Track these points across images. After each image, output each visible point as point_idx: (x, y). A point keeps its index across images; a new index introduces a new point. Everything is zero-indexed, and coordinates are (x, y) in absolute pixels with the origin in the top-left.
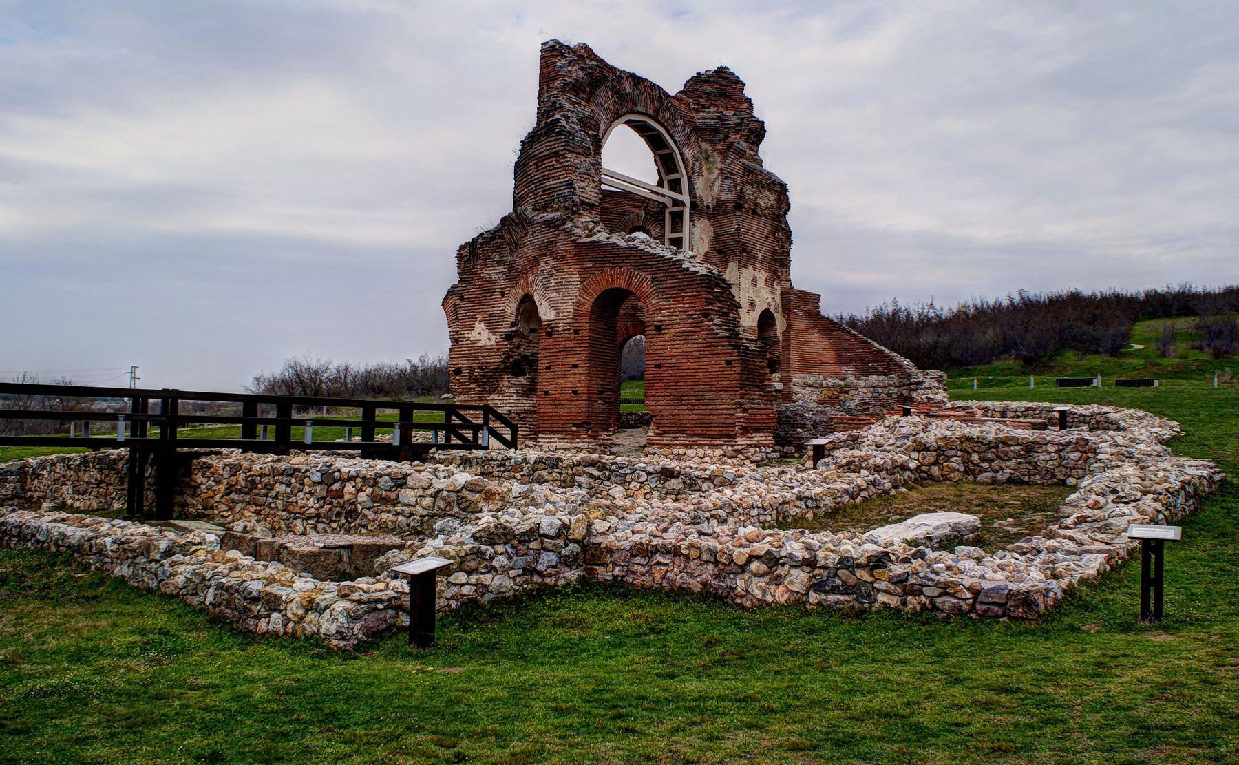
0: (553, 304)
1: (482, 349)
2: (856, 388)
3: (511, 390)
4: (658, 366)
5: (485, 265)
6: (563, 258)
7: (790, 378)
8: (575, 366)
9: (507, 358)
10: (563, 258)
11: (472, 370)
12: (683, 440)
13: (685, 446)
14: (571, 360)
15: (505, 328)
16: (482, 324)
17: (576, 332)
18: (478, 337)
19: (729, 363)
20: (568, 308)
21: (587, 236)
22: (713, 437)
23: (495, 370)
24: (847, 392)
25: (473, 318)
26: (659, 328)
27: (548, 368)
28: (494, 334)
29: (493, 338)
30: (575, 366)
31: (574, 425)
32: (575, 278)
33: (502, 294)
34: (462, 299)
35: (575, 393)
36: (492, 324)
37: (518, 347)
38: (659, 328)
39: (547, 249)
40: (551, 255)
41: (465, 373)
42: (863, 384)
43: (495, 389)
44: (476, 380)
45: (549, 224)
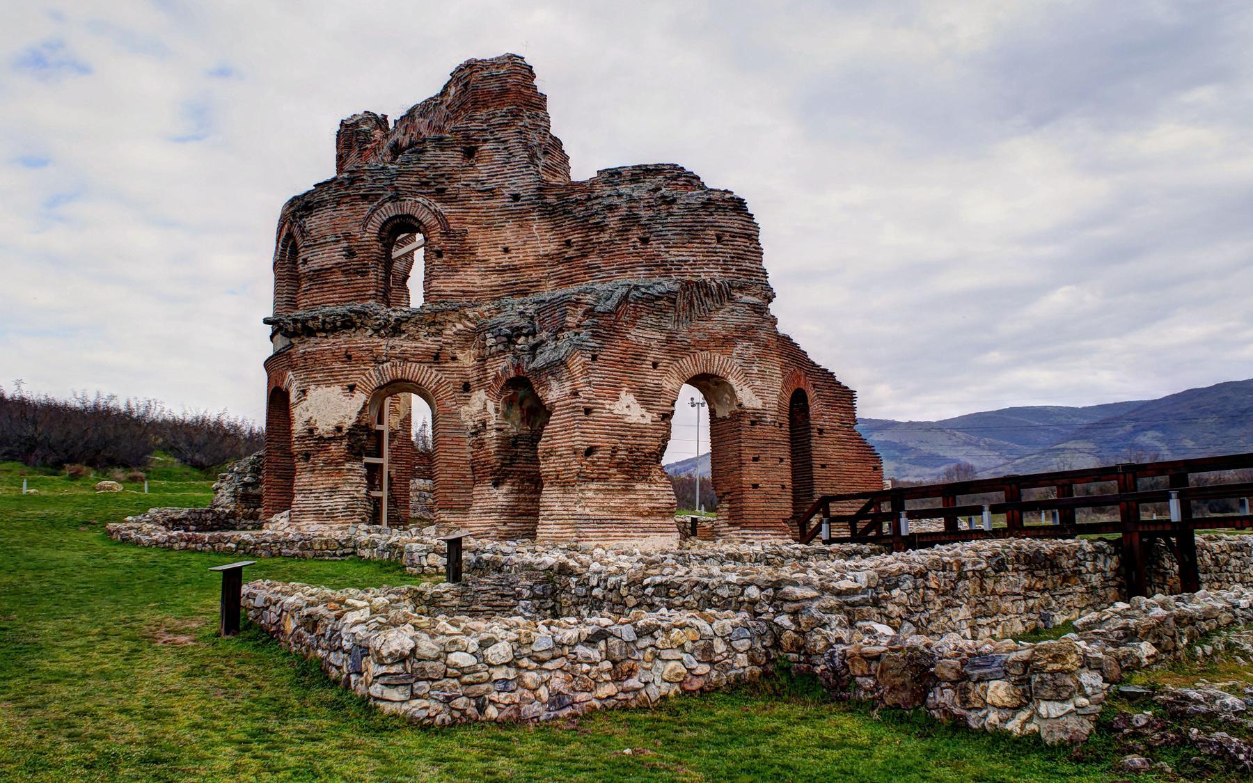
0: (758, 393)
1: (629, 427)
11: (615, 451)
14: (777, 453)
16: (631, 397)
18: (626, 411)
20: (773, 399)
25: (616, 387)
26: (821, 431)
27: (755, 459)
28: (648, 410)
29: (649, 416)
33: (655, 365)
34: (594, 358)
38: (821, 431)
39: (746, 333)
40: (750, 339)
44: (619, 465)
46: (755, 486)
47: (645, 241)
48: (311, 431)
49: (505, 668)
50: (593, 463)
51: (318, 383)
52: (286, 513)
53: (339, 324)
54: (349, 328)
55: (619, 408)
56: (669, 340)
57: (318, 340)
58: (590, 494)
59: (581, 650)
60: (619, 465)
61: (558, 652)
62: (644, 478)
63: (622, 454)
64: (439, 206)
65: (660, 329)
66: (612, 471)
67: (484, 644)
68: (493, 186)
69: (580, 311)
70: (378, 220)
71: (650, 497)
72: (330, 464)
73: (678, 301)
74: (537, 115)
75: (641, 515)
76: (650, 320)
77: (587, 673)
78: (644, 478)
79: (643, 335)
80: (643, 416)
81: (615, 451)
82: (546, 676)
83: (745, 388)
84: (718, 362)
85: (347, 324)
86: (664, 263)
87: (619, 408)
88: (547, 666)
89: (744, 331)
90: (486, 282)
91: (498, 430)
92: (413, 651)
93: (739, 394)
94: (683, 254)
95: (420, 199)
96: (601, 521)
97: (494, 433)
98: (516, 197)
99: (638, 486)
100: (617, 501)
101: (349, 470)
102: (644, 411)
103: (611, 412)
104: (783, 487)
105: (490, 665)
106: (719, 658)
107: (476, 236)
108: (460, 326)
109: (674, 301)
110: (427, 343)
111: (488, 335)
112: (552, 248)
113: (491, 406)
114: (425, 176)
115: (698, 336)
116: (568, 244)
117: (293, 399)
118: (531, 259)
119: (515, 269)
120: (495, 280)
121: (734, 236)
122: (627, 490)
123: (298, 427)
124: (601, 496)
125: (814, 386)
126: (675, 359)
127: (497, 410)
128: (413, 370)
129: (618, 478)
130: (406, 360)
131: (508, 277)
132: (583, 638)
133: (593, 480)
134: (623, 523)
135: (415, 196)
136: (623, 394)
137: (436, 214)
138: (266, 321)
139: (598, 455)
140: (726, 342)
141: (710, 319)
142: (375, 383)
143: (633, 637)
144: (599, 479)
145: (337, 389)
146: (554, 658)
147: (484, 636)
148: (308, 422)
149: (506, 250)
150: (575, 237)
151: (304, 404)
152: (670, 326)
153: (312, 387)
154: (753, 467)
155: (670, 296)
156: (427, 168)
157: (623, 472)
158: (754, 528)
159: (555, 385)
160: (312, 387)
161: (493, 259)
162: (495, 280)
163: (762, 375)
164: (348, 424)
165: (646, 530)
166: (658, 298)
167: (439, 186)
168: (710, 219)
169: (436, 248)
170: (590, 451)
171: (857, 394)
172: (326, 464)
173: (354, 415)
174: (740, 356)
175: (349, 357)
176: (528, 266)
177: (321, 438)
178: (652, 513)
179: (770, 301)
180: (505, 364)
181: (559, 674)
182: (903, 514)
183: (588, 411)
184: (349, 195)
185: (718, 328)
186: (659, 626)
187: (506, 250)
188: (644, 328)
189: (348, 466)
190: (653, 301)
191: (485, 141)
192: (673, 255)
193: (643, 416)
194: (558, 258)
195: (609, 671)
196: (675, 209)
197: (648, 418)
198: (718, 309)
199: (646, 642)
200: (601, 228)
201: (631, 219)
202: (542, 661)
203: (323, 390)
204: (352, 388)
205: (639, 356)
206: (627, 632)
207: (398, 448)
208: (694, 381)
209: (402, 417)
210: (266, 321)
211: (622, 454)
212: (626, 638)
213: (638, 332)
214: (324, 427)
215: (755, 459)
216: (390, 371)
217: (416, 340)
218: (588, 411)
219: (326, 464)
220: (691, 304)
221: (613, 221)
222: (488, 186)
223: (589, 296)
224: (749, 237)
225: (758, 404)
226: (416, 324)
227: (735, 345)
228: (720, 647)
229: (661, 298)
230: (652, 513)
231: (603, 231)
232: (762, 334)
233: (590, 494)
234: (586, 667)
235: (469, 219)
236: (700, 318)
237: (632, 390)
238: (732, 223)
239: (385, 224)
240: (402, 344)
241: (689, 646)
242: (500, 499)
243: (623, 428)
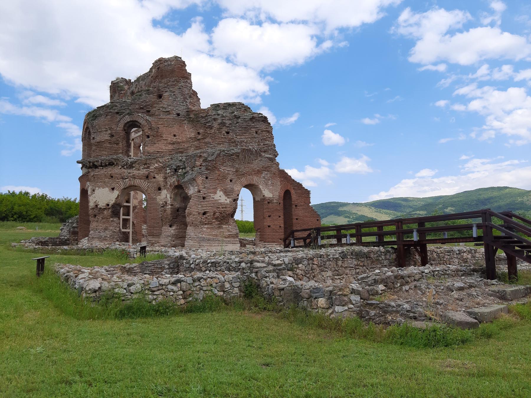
0: (271, 191)
4: (297, 219)
5: (222, 165)
11: (214, 214)
16: (222, 193)
18: (219, 198)
25: (216, 189)
26: (296, 206)
27: (269, 216)
28: (228, 198)
30: (280, 217)
32: (279, 183)
33: (231, 181)
34: (207, 178)
39: (266, 169)
40: (268, 171)
44: (216, 218)
46: (269, 226)
48: (97, 206)
49: (138, 294)
50: (206, 218)
51: (99, 187)
52: (87, 238)
53: (107, 164)
54: (112, 165)
56: (237, 171)
57: (99, 170)
58: (205, 229)
59: (170, 287)
60: (216, 218)
61: (161, 288)
62: (227, 223)
64: (148, 117)
65: (233, 167)
67: (129, 285)
68: (169, 110)
69: (201, 160)
71: (229, 231)
72: (104, 219)
74: (187, 82)
76: (230, 163)
77: (172, 295)
78: (227, 223)
79: (226, 169)
81: (214, 214)
82: (155, 297)
84: (255, 180)
85: (111, 164)
86: (235, 141)
88: (155, 293)
89: (266, 168)
90: (167, 148)
91: (171, 205)
92: (100, 288)
93: (263, 192)
94: (243, 138)
95: (140, 114)
96: (209, 240)
97: (170, 206)
98: (178, 115)
99: (224, 226)
103: (213, 198)
104: (280, 227)
105: (132, 293)
106: (227, 289)
107: (162, 129)
108: (156, 165)
109: (238, 156)
110: (143, 172)
111: (168, 169)
112: (192, 135)
113: (168, 196)
114: (142, 105)
115: (247, 169)
116: (199, 133)
117: (89, 193)
118: (184, 139)
119: (179, 143)
120: (170, 147)
121: (262, 131)
122: (220, 228)
123: (91, 204)
124: (209, 230)
125: (294, 189)
127: (171, 198)
128: (137, 182)
130: (135, 178)
131: (175, 146)
132: (171, 282)
133: (206, 224)
135: (138, 113)
136: (218, 192)
137: (147, 120)
138: (78, 162)
139: (208, 215)
140: (259, 172)
141: (252, 163)
142: (122, 187)
143: (192, 282)
144: (208, 224)
145: (107, 189)
146: (158, 290)
147: (130, 282)
148: (95, 202)
149: (175, 136)
150: (201, 131)
151: (94, 195)
152: (237, 166)
153: (97, 188)
154: (269, 219)
155: (237, 155)
158: (268, 242)
159: (192, 188)
160: (97, 188)
161: (169, 139)
162: (170, 147)
164: (111, 203)
166: (232, 155)
167: (148, 109)
168: (253, 125)
169: (147, 134)
170: (204, 213)
172: (103, 218)
174: (264, 178)
175: (112, 177)
176: (183, 142)
177: (100, 208)
178: (229, 236)
179: (276, 157)
180: (174, 180)
181: (160, 296)
182: (319, 237)
183: (204, 198)
184: (111, 112)
186: (202, 278)
187: (175, 136)
189: (111, 219)
192: (238, 139)
194: (196, 139)
195: (181, 295)
196: (239, 120)
197: (228, 201)
198: (255, 160)
199: (197, 284)
200: (211, 127)
201: (223, 124)
202: (154, 291)
203: (101, 190)
204: (113, 189)
205: (224, 177)
206: (189, 280)
207: (137, 212)
208: (246, 186)
209: (139, 200)
210: (78, 162)
211: (217, 214)
212: (188, 282)
214: (102, 205)
215: (269, 216)
216: (128, 182)
217: (139, 170)
218: (204, 198)
219: (103, 218)
221: (216, 125)
222: (167, 110)
224: (268, 132)
226: (139, 164)
227: (262, 173)
228: (227, 285)
230: (229, 236)
232: (273, 169)
233: (205, 229)
234: (172, 293)
235: (160, 123)
237: (222, 190)
238: (263, 126)
239: (126, 124)
240: (134, 171)
241: (214, 285)
242: (172, 231)
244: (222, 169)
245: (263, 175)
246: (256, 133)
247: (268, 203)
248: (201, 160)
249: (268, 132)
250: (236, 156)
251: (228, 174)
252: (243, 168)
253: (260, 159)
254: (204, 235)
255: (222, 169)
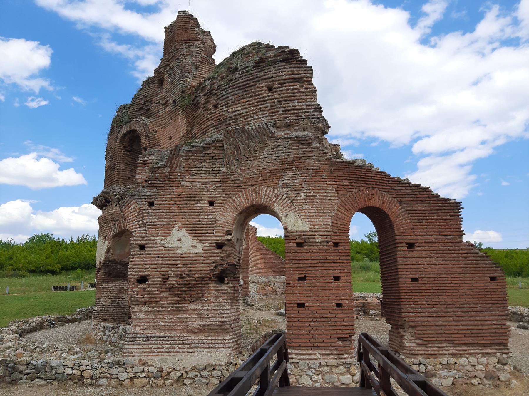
2: (274, 283)
3: (220, 300)
4: (414, 280)
5: (188, 172)
6: (317, 173)
7: (248, 277)
8: (337, 278)
9: (216, 267)
10: (317, 173)
11: (165, 278)
12: (451, 350)
13: (453, 355)
14: (332, 272)
15: (219, 236)
16: (184, 232)
17: (336, 245)
18: (177, 244)
19: (493, 279)
21: (335, 157)
22: (484, 346)
23: (202, 278)
24: (269, 286)
26: (411, 246)
27: (302, 279)
28: (201, 241)
30: (337, 278)
31: (339, 339)
32: (333, 193)
33: (211, 204)
35: (339, 305)
36: (196, 231)
37: (228, 256)
38: (411, 246)
40: (298, 169)
41: (155, 281)
42: (277, 281)
43: (198, 299)
44: (171, 289)
45: (300, 140)
47: (216, 106)
50: (145, 289)
55: (170, 242)
56: (224, 181)
58: (141, 315)
60: (171, 289)
63: (172, 281)
64: (146, 121)
65: (216, 173)
66: (162, 295)
69: (147, 169)
70: (120, 136)
71: (202, 317)
73: (226, 148)
75: (192, 332)
76: (206, 167)
80: (194, 247)
81: (165, 278)
83: (291, 213)
87: (170, 242)
89: (292, 162)
95: (138, 119)
99: (192, 306)
100: (167, 321)
101: (104, 288)
102: (195, 242)
103: (162, 245)
109: (222, 148)
121: (282, 83)
122: (177, 310)
125: (401, 202)
126: (230, 196)
129: (168, 300)
133: (145, 303)
134: (170, 339)
135: (136, 118)
136: (175, 231)
140: (273, 176)
141: (256, 158)
144: (151, 303)
152: (224, 170)
156: (142, 99)
157: (176, 295)
158: (299, 347)
163: (311, 199)
165: (192, 346)
166: (205, 149)
169: (144, 146)
171: (463, 205)
173: (104, 255)
174: (286, 185)
178: (203, 330)
179: (324, 133)
185: (265, 164)
188: (198, 174)
189: (104, 285)
190: (201, 152)
191: (167, 72)
192: (230, 112)
193: (194, 247)
198: (262, 148)
205: (193, 198)
211: (172, 281)
213: (192, 179)
215: (302, 279)
220: (237, 148)
223: (153, 157)
224: (299, 80)
225: (305, 226)
227: (281, 177)
229: (208, 148)
230: (203, 330)
231: (199, 108)
232: (312, 163)
235: (158, 124)
236: (248, 159)
237: (186, 227)
243: (175, 258)
244: (187, 181)
245: (284, 180)
246: (270, 89)
247: (300, 245)
248: (147, 169)
249: (299, 80)
250: (216, 148)
251: (201, 189)
252: (238, 173)
253: (271, 144)
254: (138, 329)
255: (187, 181)
